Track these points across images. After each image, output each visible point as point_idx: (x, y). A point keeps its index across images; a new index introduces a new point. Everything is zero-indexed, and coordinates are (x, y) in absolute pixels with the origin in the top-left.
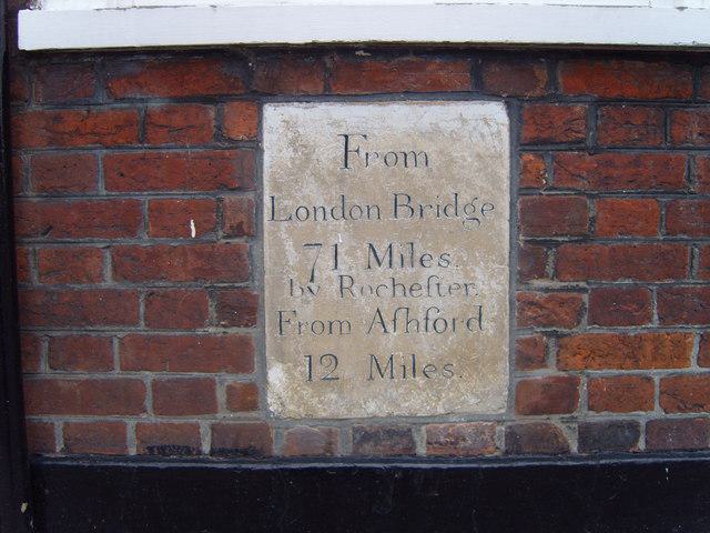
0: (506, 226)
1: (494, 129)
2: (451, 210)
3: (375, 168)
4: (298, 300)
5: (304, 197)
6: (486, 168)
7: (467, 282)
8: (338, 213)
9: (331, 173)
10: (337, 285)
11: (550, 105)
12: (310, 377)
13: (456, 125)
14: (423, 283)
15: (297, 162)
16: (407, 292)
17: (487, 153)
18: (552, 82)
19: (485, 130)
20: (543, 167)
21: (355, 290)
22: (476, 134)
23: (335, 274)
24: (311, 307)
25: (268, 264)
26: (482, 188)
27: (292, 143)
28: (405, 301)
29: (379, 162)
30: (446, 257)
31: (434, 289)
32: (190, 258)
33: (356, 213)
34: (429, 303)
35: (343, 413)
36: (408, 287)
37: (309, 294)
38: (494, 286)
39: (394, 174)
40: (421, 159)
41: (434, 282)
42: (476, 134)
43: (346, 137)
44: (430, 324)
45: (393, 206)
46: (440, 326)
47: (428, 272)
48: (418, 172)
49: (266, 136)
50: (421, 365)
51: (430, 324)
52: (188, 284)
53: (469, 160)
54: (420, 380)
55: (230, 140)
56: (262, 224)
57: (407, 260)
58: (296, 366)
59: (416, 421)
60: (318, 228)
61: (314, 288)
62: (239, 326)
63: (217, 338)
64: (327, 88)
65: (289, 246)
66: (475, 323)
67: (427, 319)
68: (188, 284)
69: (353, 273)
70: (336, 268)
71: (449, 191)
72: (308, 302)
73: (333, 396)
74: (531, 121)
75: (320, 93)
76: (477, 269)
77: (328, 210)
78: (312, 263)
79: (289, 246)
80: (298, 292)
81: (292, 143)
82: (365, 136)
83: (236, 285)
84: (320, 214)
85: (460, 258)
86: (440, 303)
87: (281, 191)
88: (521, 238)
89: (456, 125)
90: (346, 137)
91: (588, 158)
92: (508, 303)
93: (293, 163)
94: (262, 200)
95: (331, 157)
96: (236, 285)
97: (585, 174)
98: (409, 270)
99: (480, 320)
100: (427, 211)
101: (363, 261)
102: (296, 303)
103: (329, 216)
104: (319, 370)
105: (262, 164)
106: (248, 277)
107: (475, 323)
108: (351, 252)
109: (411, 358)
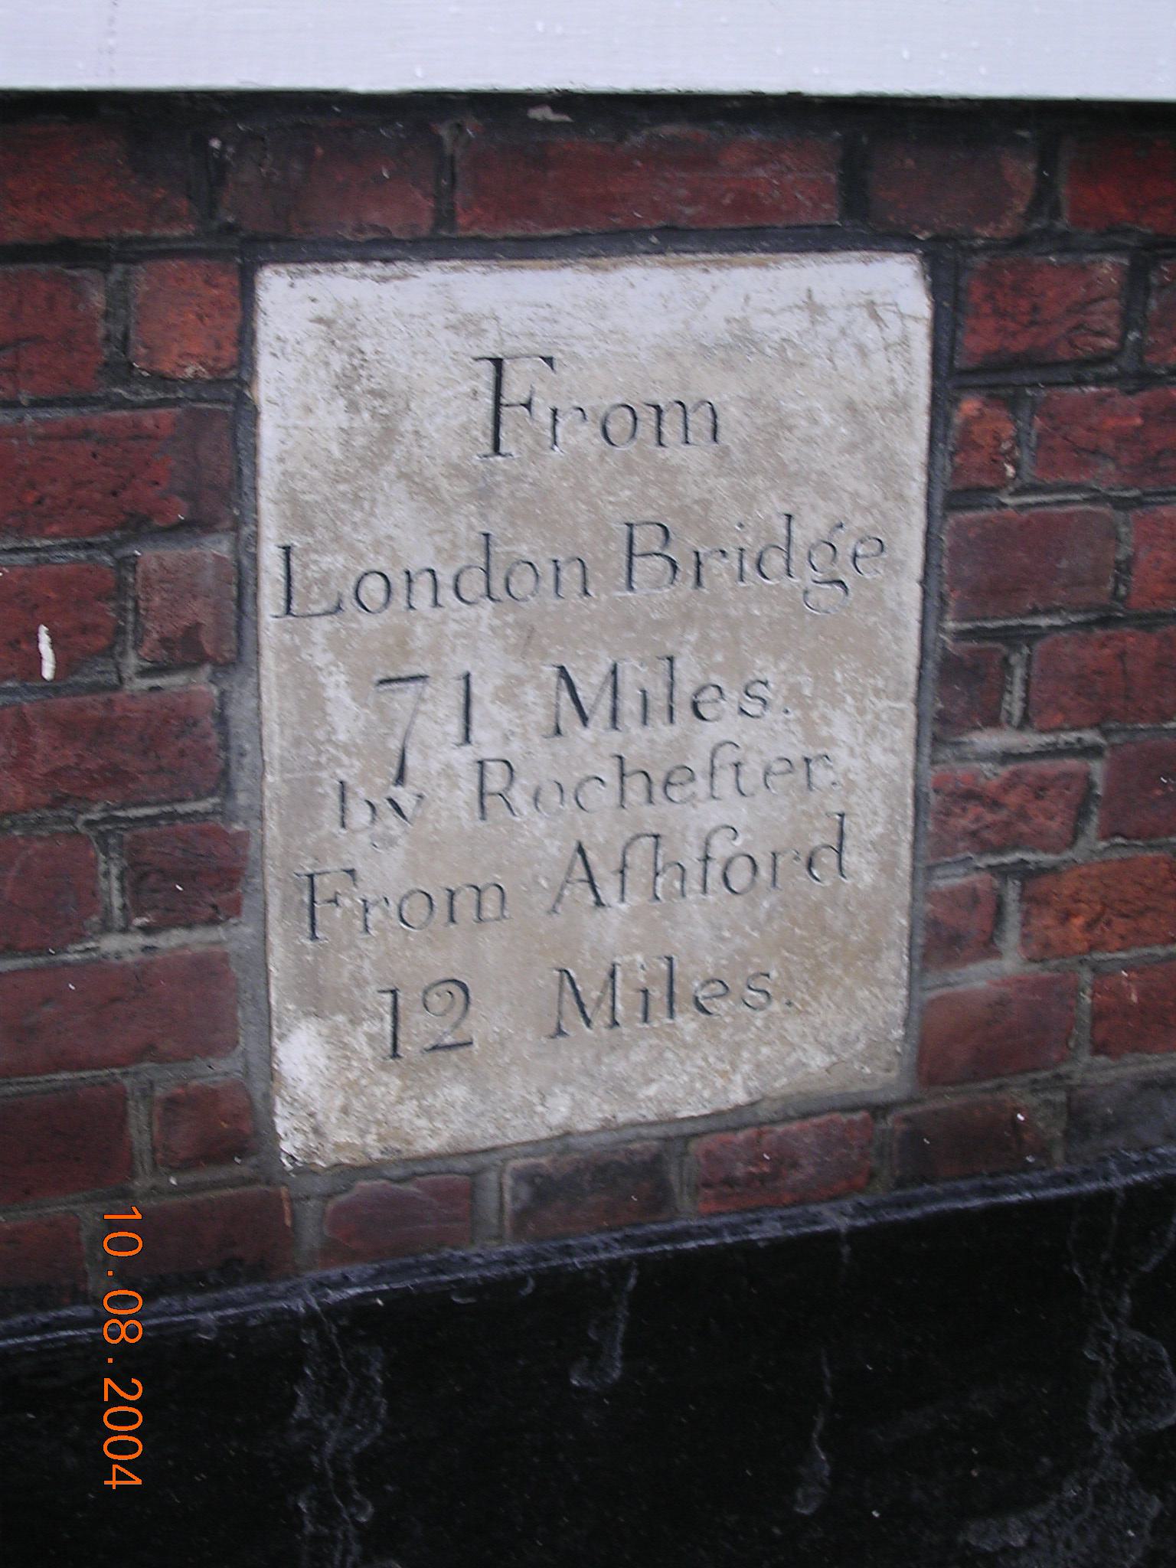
0: (912, 594)
1: (894, 332)
2: (775, 562)
3: (578, 455)
4: (364, 838)
5: (377, 546)
6: (869, 439)
7: (811, 752)
8: (474, 584)
9: (457, 471)
10: (468, 788)
11: (1037, 260)
12: (395, 1046)
13: (793, 324)
14: (698, 764)
15: (360, 441)
16: (657, 790)
17: (872, 401)
18: (1043, 198)
19: (870, 334)
20: (1010, 430)
21: (520, 798)
22: (845, 346)
23: (463, 759)
24: (398, 854)
25: (276, 744)
26: (855, 495)
27: (345, 383)
28: (650, 817)
29: (587, 436)
30: (759, 690)
31: (725, 778)
32: (41, 740)
33: (522, 583)
34: (713, 815)
35: (484, 1133)
36: (658, 776)
37: (392, 820)
38: (878, 756)
39: (629, 467)
40: (700, 421)
41: (727, 755)
42: (845, 346)
43: (498, 363)
44: (715, 870)
45: (624, 558)
46: (740, 876)
47: (711, 733)
48: (695, 457)
49: (267, 366)
50: (691, 982)
51: (715, 870)
52: (34, 815)
53: (827, 419)
54: (687, 1023)
55: (161, 380)
56: (256, 625)
57: (658, 703)
58: (355, 1022)
59: (672, 1131)
60: (419, 629)
61: (405, 797)
62: (189, 926)
63: (124, 968)
64: (445, 217)
65: (337, 686)
66: (829, 859)
67: (707, 859)
68: (34, 815)
69: (515, 750)
70: (467, 739)
71: (772, 507)
72: (392, 842)
73: (459, 1092)
74: (986, 309)
75: (425, 231)
76: (837, 716)
77: (445, 578)
78: (399, 731)
79: (337, 686)
80: (360, 815)
81: (345, 383)
82: (549, 360)
83: (182, 808)
84: (423, 588)
85: (795, 690)
86: (739, 813)
87: (309, 528)
88: (950, 625)
89: (793, 324)
90: (498, 363)
91: (1121, 401)
92: (909, 801)
93: (346, 445)
94: (255, 558)
95: (454, 423)
96: (182, 808)
97: (1109, 444)
98: (662, 731)
99: (840, 853)
100: (715, 566)
101: (540, 715)
102: (356, 850)
103: (447, 595)
104: (420, 1028)
105: (254, 450)
106: (223, 784)
107: (829, 859)
108: (508, 695)
109: (664, 967)
